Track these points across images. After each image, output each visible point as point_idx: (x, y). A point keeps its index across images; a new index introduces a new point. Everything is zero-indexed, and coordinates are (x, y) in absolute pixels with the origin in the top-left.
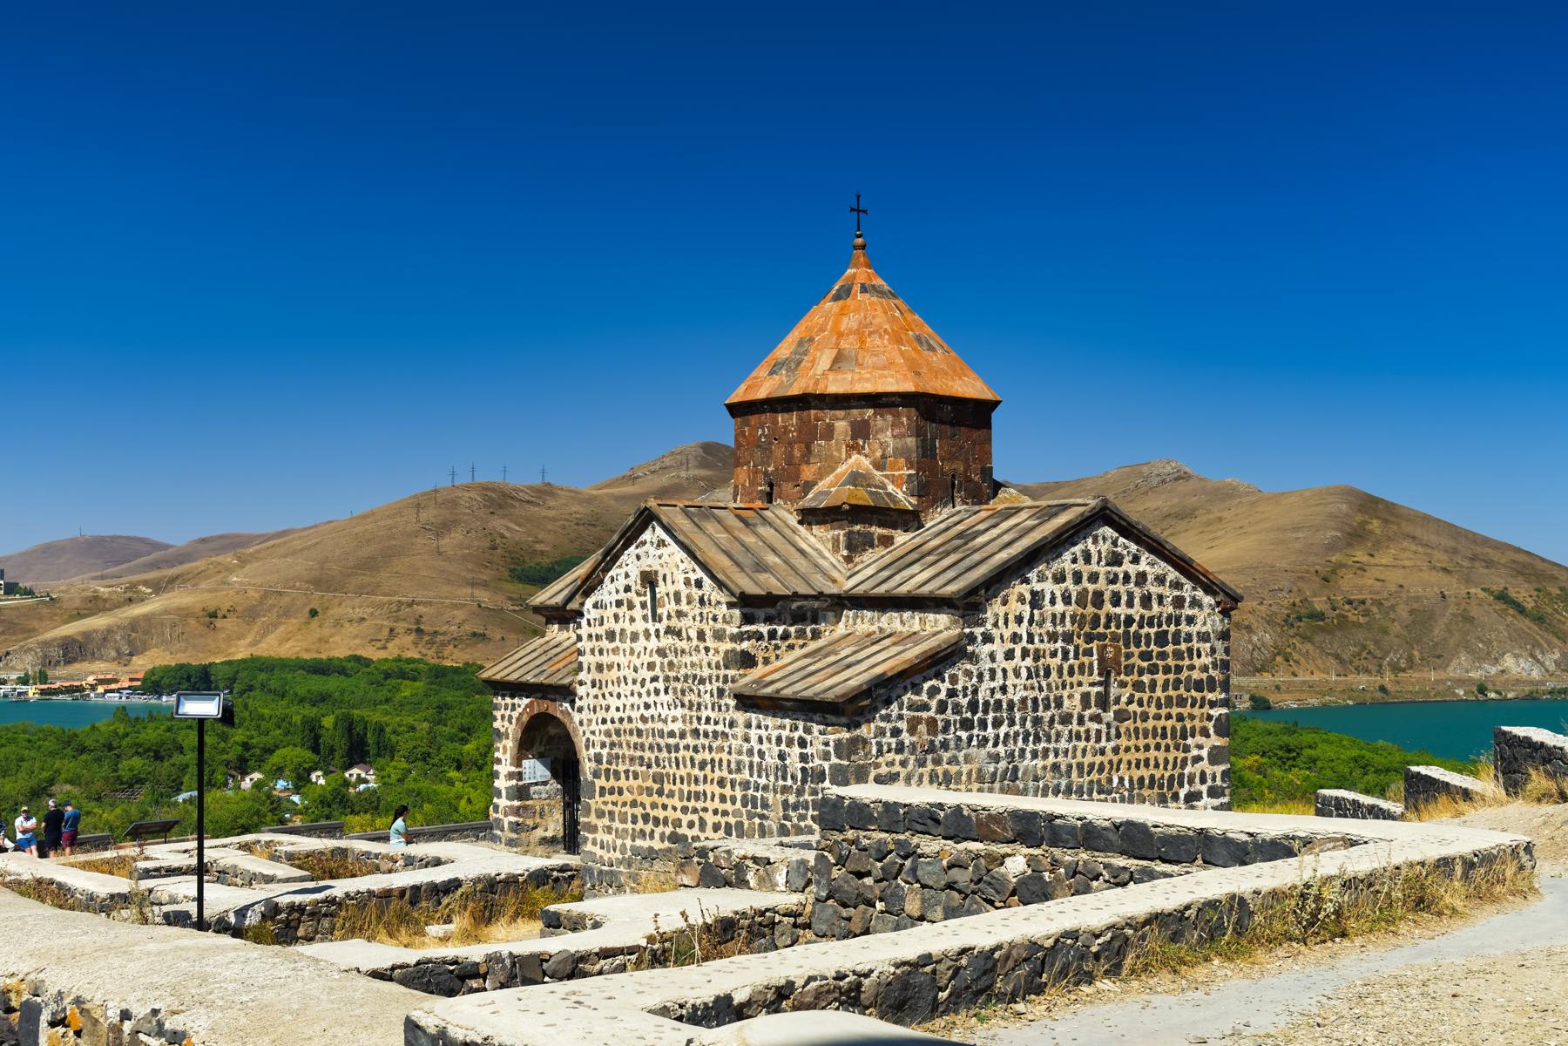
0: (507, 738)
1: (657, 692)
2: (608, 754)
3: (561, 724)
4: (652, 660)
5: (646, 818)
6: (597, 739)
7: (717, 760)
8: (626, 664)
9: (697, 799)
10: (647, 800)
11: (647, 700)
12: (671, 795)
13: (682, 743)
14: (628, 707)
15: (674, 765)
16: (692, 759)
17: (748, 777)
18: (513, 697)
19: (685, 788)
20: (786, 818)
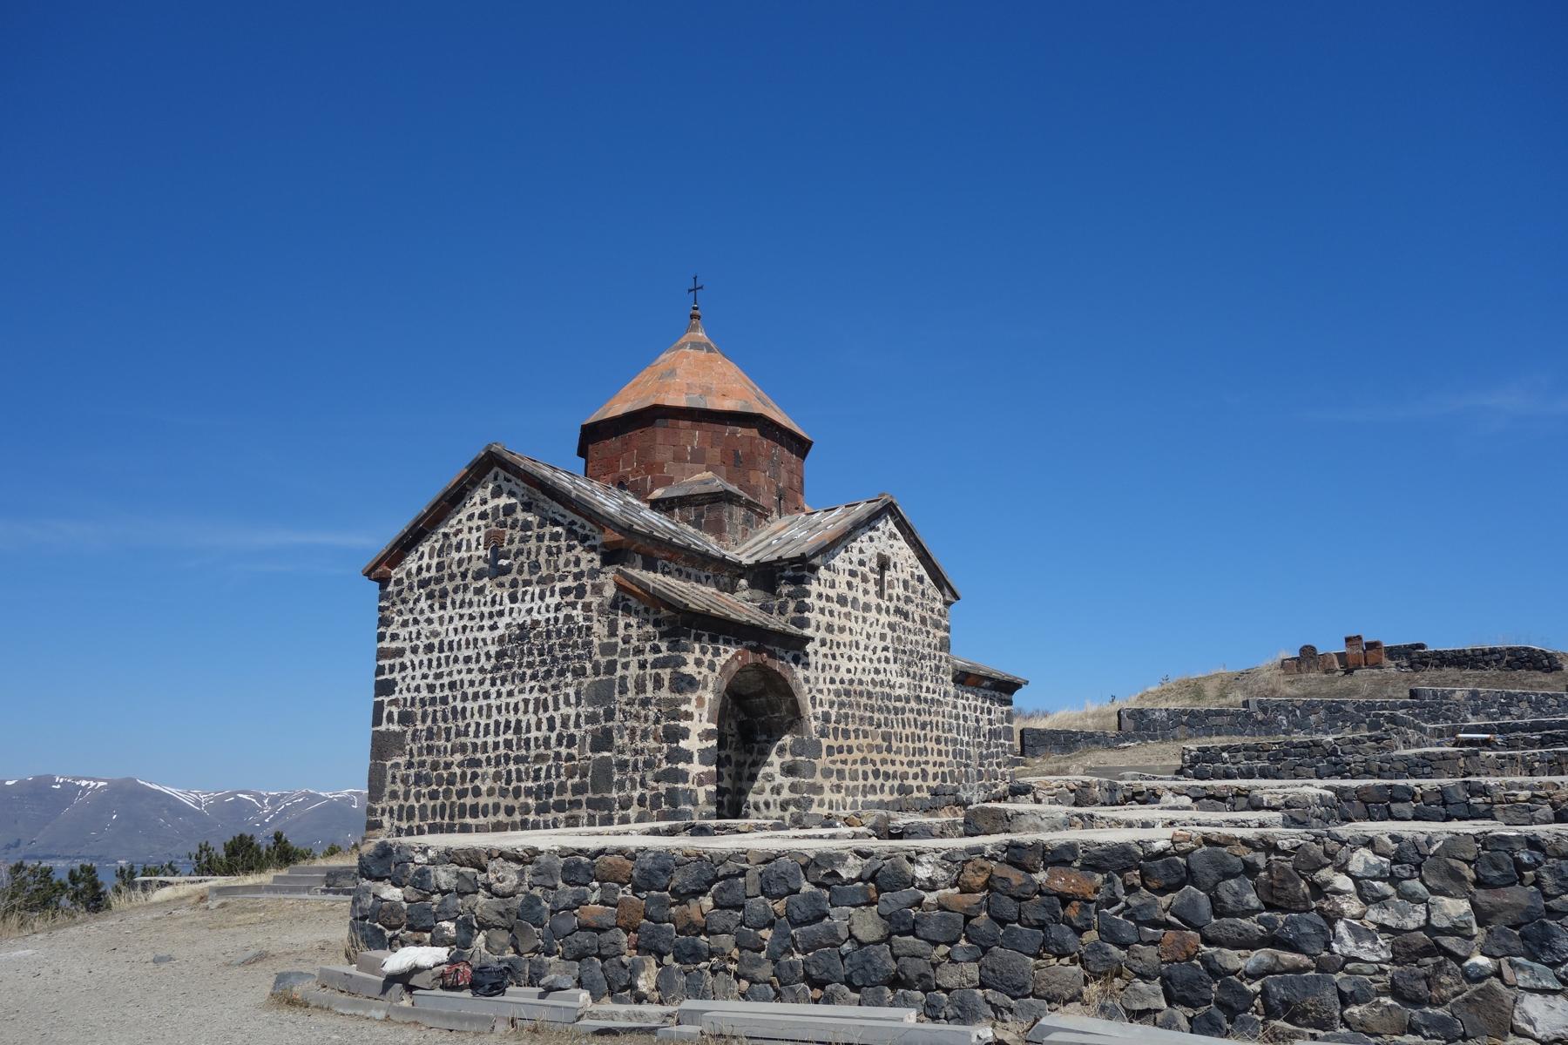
0: (705, 687)
2: (837, 713)
3: (785, 680)
4: (884, 631)
5: (876, 774)
6: (825, 697)
7: (934, 723)
8: (859, 631)
9: (920, 754)
12: (898, 752)
13: (908, 706)
14: (859, 670)
15: (900, 725)
16: (915, 720)
18: (713, 640)
19: (910, 744)
20: (981, 765)
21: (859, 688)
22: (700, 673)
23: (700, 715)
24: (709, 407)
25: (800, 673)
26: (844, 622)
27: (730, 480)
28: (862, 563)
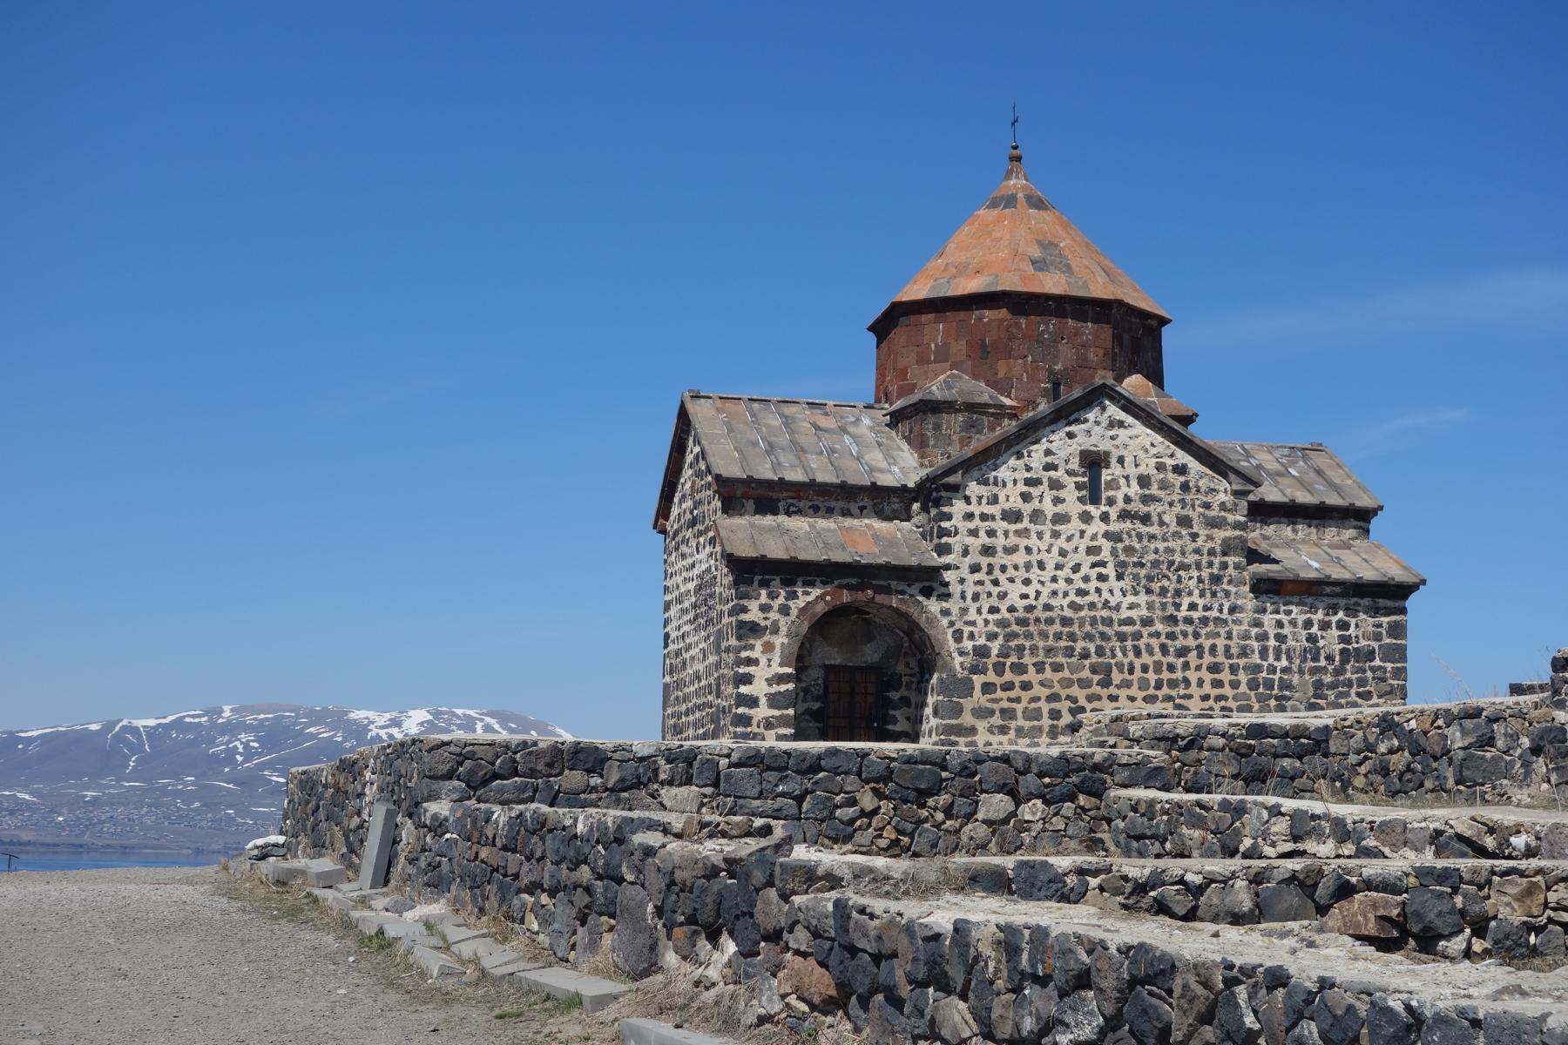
0: (775, 631)
1: (1102, 578)
4: (1095, 543)
8: (1044, 547)
10: (1080, 694)
11: (1083, 586)
12: (1127, 684)
15: (1131, 654)
17: (1259, 661)
19: (1152, 676)
20: (1316, 696)
21: (1044, 615)
22: (765, 619)
23: (769, 660)
24: (950, 293)
25: (934, 606)
26: (1023, 542)
27: (975, 376)
28: (1049, 467)
